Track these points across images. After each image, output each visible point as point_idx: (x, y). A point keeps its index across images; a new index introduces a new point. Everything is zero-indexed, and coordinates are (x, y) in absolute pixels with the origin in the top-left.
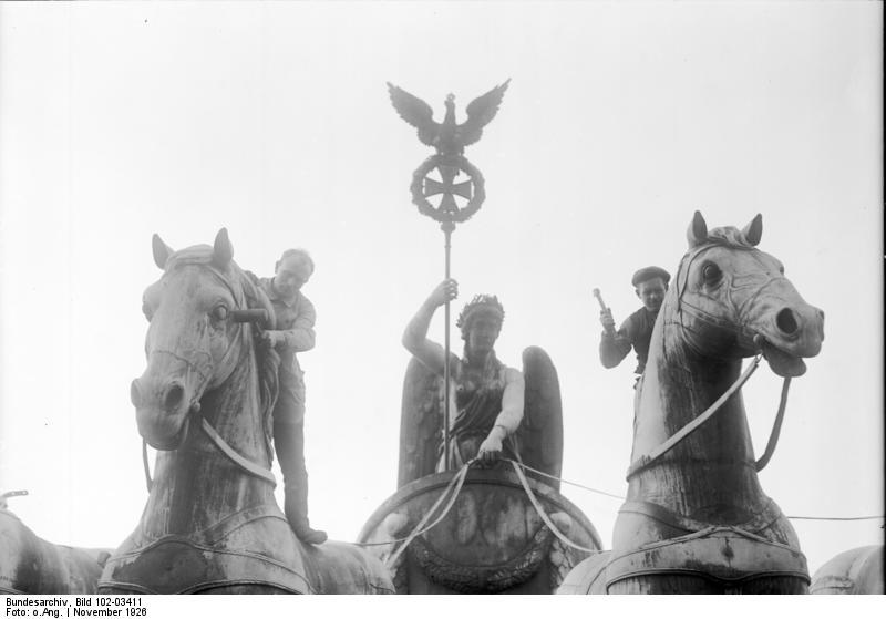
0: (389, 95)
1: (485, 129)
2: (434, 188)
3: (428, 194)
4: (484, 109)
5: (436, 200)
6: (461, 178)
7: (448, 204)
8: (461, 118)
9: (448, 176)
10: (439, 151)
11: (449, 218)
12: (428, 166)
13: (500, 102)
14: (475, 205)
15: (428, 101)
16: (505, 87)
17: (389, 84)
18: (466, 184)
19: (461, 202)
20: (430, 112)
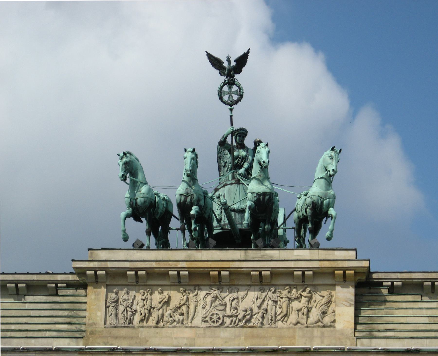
1: (244, 69)
4: (242, 61)
5: (226, 98)
6: (235, 88)
8: (233, 63)
9: (230, 88)
10: (227, 77)
11: (231, 104)
12: (224, 84)
13: (248, 58)
16: (248, 52)
17: (206, 52)
18: (237, 91)
19: (235, 97)
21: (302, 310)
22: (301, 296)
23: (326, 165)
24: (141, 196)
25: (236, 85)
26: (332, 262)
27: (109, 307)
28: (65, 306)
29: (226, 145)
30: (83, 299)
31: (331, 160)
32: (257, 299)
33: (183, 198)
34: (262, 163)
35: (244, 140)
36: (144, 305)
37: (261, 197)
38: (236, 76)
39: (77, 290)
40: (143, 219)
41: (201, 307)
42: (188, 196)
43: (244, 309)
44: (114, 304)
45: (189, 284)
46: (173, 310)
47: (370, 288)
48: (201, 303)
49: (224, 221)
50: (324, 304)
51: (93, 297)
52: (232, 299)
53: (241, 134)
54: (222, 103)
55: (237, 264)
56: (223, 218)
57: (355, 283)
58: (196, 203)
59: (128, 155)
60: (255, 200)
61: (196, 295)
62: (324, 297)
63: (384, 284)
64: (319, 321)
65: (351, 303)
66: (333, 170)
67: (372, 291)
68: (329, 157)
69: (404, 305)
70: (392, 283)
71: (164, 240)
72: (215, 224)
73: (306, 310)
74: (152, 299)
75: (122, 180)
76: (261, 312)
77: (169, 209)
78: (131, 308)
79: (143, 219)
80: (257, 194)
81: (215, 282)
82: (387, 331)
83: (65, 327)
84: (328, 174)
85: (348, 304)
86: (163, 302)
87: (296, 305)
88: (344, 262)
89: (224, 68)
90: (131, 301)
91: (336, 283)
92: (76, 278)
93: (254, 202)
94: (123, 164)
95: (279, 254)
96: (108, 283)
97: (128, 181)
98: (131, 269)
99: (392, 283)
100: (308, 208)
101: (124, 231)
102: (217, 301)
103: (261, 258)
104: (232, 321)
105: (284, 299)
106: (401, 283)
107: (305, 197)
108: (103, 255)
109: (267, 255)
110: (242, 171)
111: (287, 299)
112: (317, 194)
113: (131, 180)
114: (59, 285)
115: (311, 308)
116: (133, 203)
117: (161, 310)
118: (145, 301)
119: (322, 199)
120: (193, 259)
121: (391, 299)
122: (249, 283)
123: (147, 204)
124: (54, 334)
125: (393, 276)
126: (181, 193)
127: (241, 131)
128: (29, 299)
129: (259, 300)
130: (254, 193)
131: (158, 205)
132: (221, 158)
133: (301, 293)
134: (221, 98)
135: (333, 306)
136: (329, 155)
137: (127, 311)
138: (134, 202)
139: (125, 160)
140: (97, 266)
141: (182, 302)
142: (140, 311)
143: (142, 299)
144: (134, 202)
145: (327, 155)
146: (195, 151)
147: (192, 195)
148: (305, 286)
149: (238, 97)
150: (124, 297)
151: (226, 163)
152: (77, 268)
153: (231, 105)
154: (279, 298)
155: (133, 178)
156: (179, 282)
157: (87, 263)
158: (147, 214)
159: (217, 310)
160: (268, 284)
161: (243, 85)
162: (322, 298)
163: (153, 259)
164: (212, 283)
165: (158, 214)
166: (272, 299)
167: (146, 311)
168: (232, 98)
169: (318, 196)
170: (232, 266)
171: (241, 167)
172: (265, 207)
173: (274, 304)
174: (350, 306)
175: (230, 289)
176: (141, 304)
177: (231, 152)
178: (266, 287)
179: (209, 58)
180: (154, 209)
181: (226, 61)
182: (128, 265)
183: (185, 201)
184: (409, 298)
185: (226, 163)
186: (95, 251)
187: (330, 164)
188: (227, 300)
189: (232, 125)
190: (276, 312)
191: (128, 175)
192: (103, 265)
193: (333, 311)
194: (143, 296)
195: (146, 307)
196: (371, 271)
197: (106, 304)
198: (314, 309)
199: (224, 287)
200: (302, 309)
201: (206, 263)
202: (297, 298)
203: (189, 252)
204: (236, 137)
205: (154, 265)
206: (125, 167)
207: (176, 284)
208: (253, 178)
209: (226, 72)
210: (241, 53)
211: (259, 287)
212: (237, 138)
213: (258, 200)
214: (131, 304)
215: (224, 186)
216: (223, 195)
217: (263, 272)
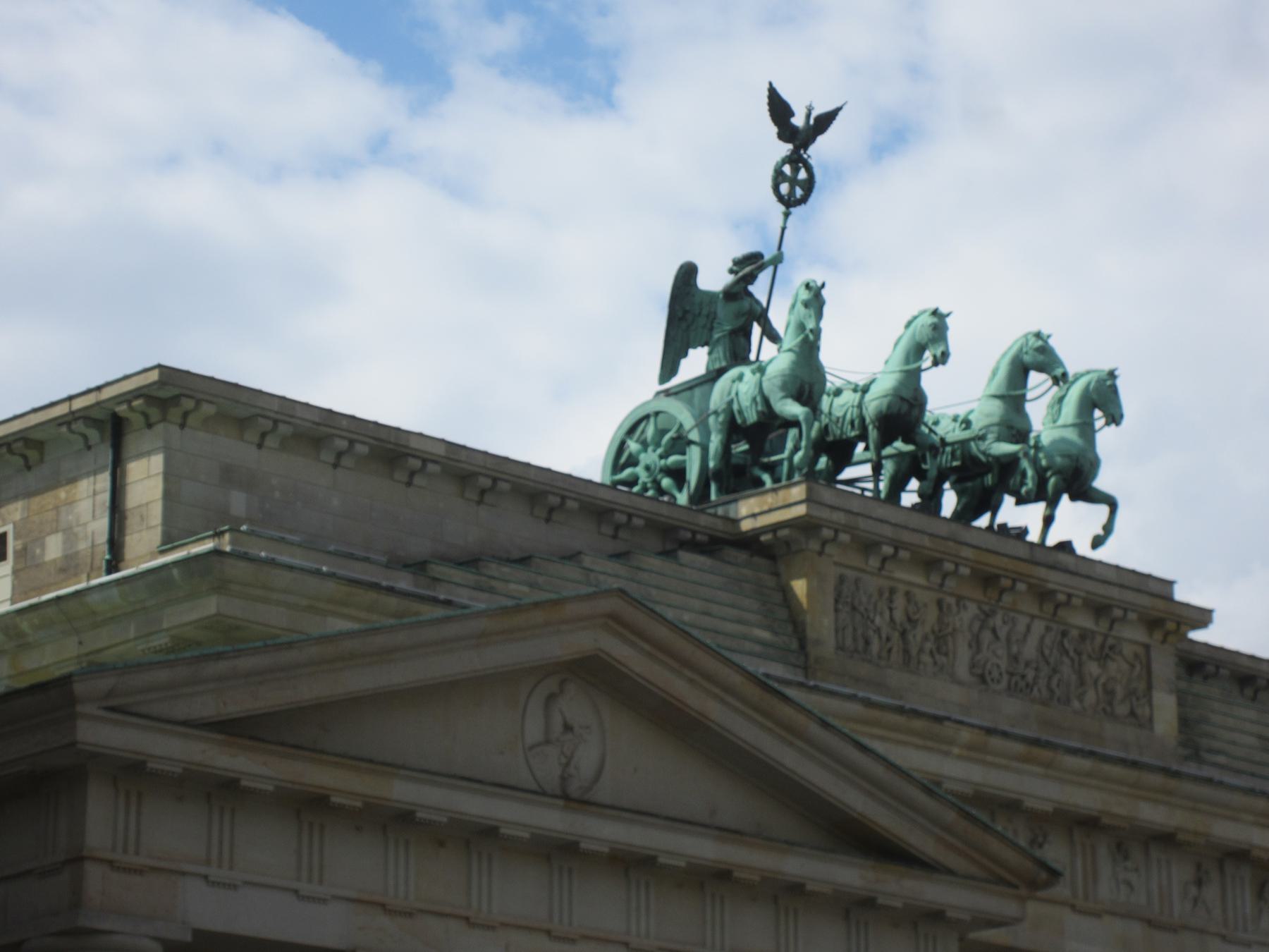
0: (767, 93)
4: (824, 122)
5: (784, 188)
6: (802, 175)
8: (812, 122)
14: (803, 200)
15: (794, 107)
17: (771, 84)
20: (792, 114)
22: (1107, 656)
33: (905, 408)
54: (774, 199)
64: (1132, 713)
82: (1218, 752)
83: (765, 635)
89: (794, 129)
104: (1016, 684)
122: (1036, 612)
124: (757, 648)
128: (685, 556)
134: (776, 189)
144: (807, 387)
151: (686, 312)
156: (942, 585)
178: (1054, 626)
182: (887, 531)
205: (926, 541)
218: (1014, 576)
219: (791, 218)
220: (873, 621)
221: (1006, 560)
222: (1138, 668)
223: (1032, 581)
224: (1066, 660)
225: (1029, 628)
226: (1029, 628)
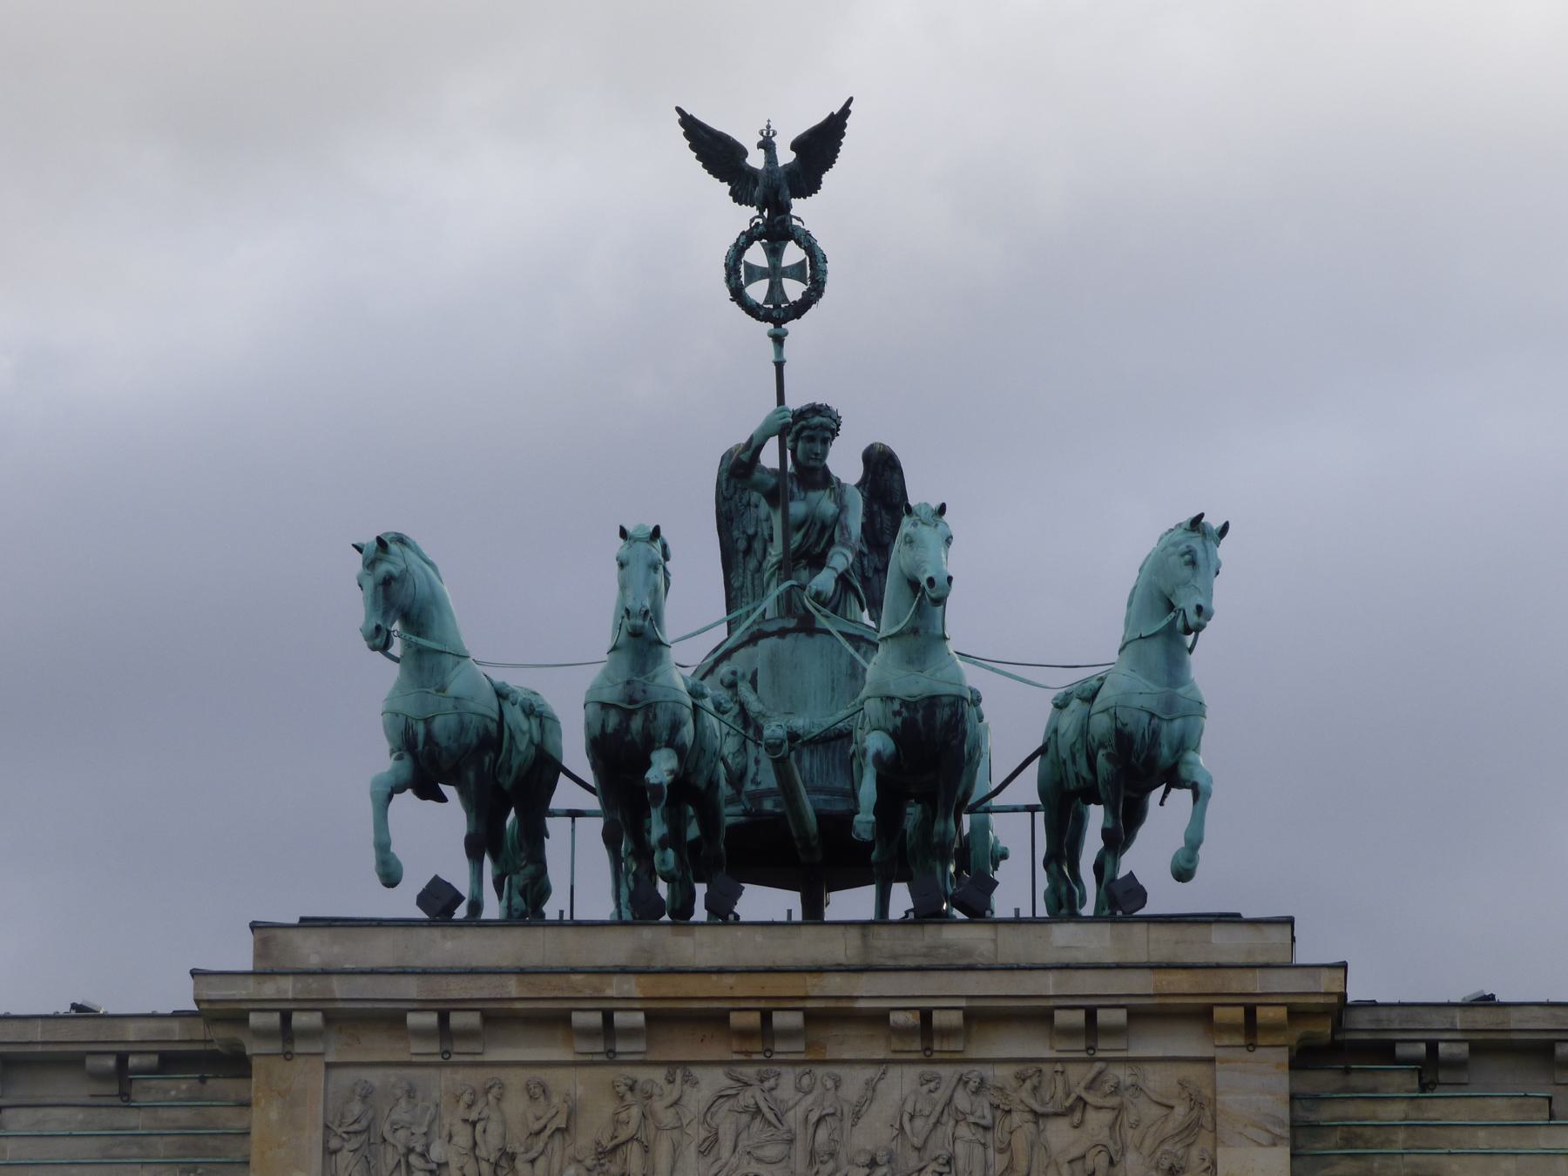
1: (826, 177)
2: (754, 273)
3: (750, 280)
4: (821, 145)
5: (758, 291)
6: (793, 254)
7: (775, 291)
8: (786, 156)
9: (774, 253)
10: (761, 213)
11: (778, 314)
12: (748, 238)
16: (845, 112)
17: (679, 110)
18: (802, 264)
19: (794, 290)
20: (745, 153)
21: (1089, 1164)
22: (1082, 1103)
23: (1167, 590)
24: (449, 704)
25: (798, 243)
26: (1200, 976)
27: (335, 1152)
28: (161, 1147)
29: (757, 476)
30: (230, 1119)
31: (1187, 571)
32: (912, 1117)
33: (613, 720)
34: (924, 583)
35: (825, 454)
36: (475, 1144)
37: (919, 716)
38: (799, 207)
39: (203, 1080)
40: (449, 791)
41: (693, 1148)
42: (633, 712)
43: (864, 1159)
44: (354, 1143)
45: (649, 1058)
46: (589, 1162)
47: (1347, 1071)
48: (698, 1133)
49: (754, 781)
50: (1173, 1136)
51: (274, 1115)
52: (813, 1117)
53: (810, 428)
55: (835, 984)
56: (752, 769)
57: (1290, 1050)
58: (665, 736)
59: (394, 547)
60: (896, 727)
61: (675, 1103)
62: (1172, 1108)
63: (1400, 1050)
65: (1278, 1131)
66: (1199, 609)
67: (1356, 1080)
68: (1183, 555)
69: (1482, 1138)
70: (1432, 1046)
71: (530, 869)
72: (725, 790)
73: (1102, 1160)
74: (504, 1122)
75: (374, 648)
76: (930, 1169)
77: (550, 747)
78: (423, 1155)
79: (449, 791)
80: (904, 703)
81: (747, 1053)
84: (1180, 624)
85: (1264, 1137)
86: (548, 1132)
87: (1059, 1134)
88: (1249, 974)
90: (425, 1129)
91: (1220, 1053)
92: (199, 1030)
93: (894, 735)
94: (376, 587)
95: (995, 941)
96: (331, 1058)
97: (396, 648)
98: (423, 1006)
99: (1432, 1046)
100: (1101, 752)
101: (383, 848)
102: (757, 1124)
103: (925, 955)
105: (1016, 1118)
106: (1465, 1047)
107: (1086, 706)
108: (313, 950)
109: (947, 947)
110: (825, 581)
111: (1029, 1117)
112: (1138, 702)
113: (408, 645)
114: (133, 1061)
115: (1123, 1151)
116: (415, 735)
117: (541, 1163)
118: (479, 1127)
119: (1155, 721)
120: (659, 963)
121: (1432, 1115)
122: (881, 1055)
123: (472, 738)
125: (1437, 1020)
126: (607, 697)
127: (817, 420)
129: (919, 1122)
130: (891, 698)
131: (512, 737)
132: (731, 520)
133: (1084, 1095)
134: (738, 295)
135: (1205, 1140)
136: (1183, 548)
137: (408, 1163)
138: (420, 729)
139: (383, 568)
140: (290, 996)
141: (622, 1137)
142: (461, 1168)
143: (465, 1121)
144: (420, 729)
145: (1171, 549)
146: (663, 533)
147: (650, 708)
148: (1098, 1066)
149: (804, 288)
150: (394, 1117)
151: (751, 539)
152: (209, 1001)
153: (778, 323)
154: (999, 1113)
155: (414, 638)
156: (611, 1052)
157: (251, 981)
158: (471, 775)
159: (759, 1160)
160: (958, 1056)
161: (822, 244)
162: (1164, 1111)
163: (506, 963)
164: (736, 1057)
165: (509, 771)
166: (971, 1119)
167: (484, 1166)
168: (783, 292)
169: (1141, 709)
170: (816, 993)
171: (818, 563)
172: (935, 746)
173: (980, 1135)
174: (1274, 1145)
175: (806, 1081)
176: (463, 1138)
177: (776, 496)
178: (948, 1073)
179: (685, 135)
180: (498, 752)
181: (760, 145)
182: (410, 988)
183: (624, 727)
184: (1501, 1110)
185: (751, 539)
186: (279, 932)
187: (1185, 583)
188: (793, 1118)
189: (781, 399)
190: (986, 1166)
191: (397, 626)
192: (315, 987)
193: (1207, 1164)
194: (469, 1107)
195: (482, 1152)
196: (1350, 999)
197: (326, 1142)
198: (1132, 1157)
199: (783, 1069)
200: (1089, 1157)
201: (714, 977)
202: (1069, 1111)
203: (647, 934)
204: (796, 440)
205: (512, 987)
206: (387, 597)
207: (597, 1058)
208: (884, 639)
209: (758, 192)
210: (817, 117)
211: (919, 1069)
212: (800, 445)
213: (909, 724)
214: (423, 1140)
215: (754, 638)
216: (749, 677)
217: (935, 1014)
218: (762, 1004)
219: (787, 340)
220: (423, 1155)
221: (729, 980)
222: (1181, 1110)
223: (810, 1004)
224: (964, 1131)
225: (871, 1086)
226: (871, 1086)
